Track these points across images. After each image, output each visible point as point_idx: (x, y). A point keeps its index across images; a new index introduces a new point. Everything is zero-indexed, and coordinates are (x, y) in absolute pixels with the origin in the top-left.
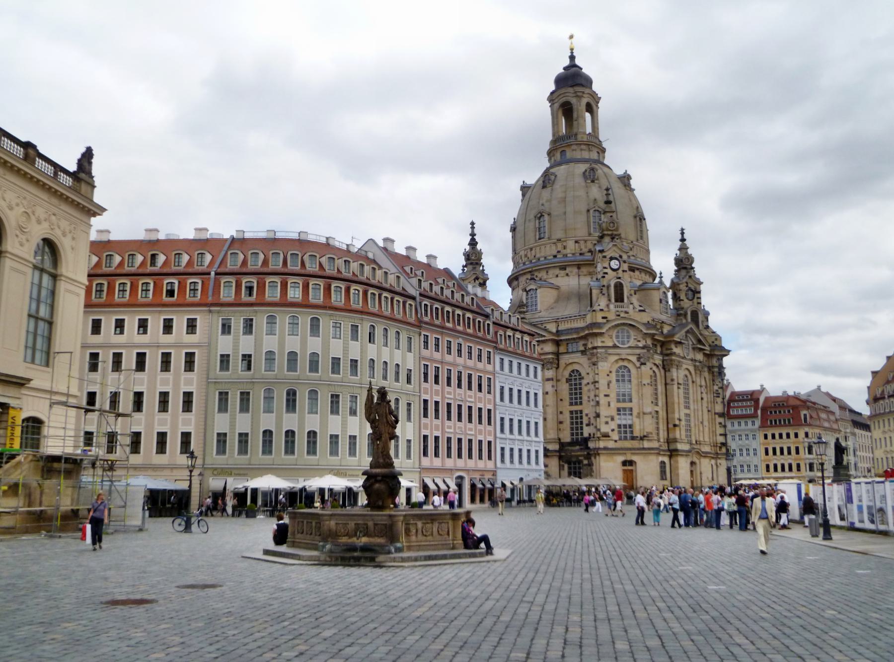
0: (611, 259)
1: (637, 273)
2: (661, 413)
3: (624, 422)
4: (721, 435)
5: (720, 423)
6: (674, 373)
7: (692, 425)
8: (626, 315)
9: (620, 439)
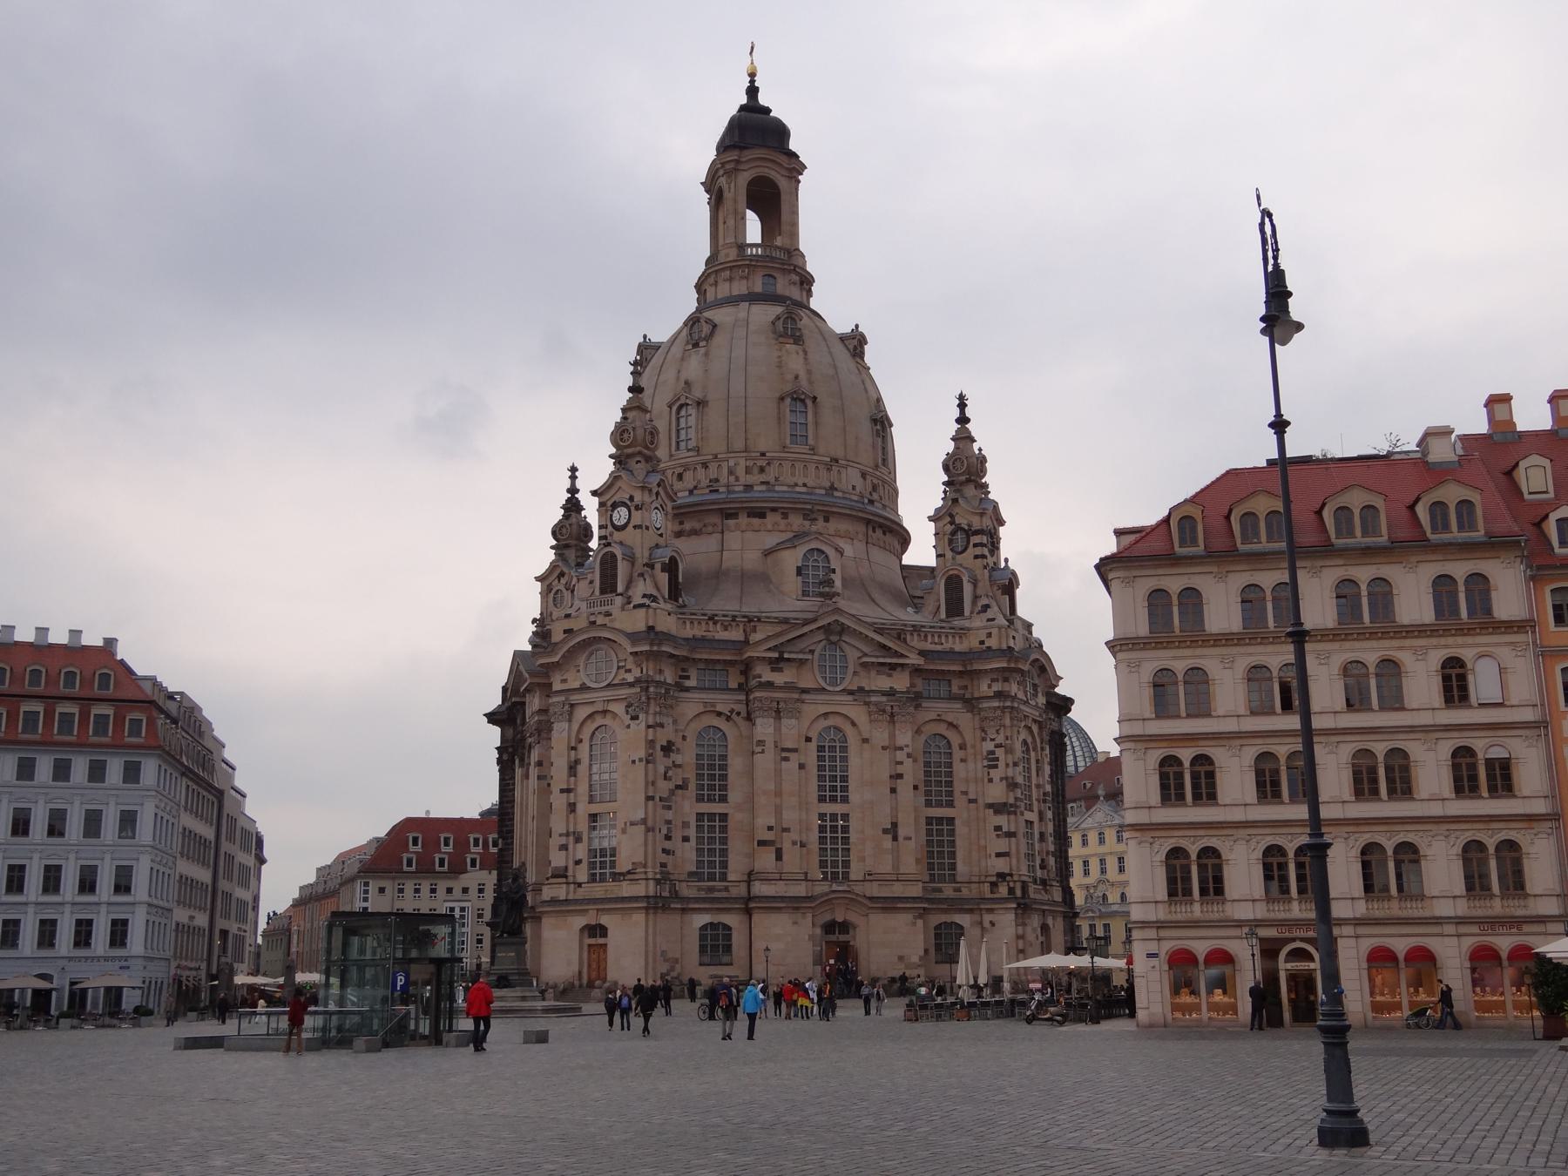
0: (615, 506)
1: (771, 518)
2: (737, 818)
3: (605, 844)
4: (998, 855)
5: (998, 828)
6: (764, 728)
7: (853, 836)
8: (606, 620)
9: (593, 879)
